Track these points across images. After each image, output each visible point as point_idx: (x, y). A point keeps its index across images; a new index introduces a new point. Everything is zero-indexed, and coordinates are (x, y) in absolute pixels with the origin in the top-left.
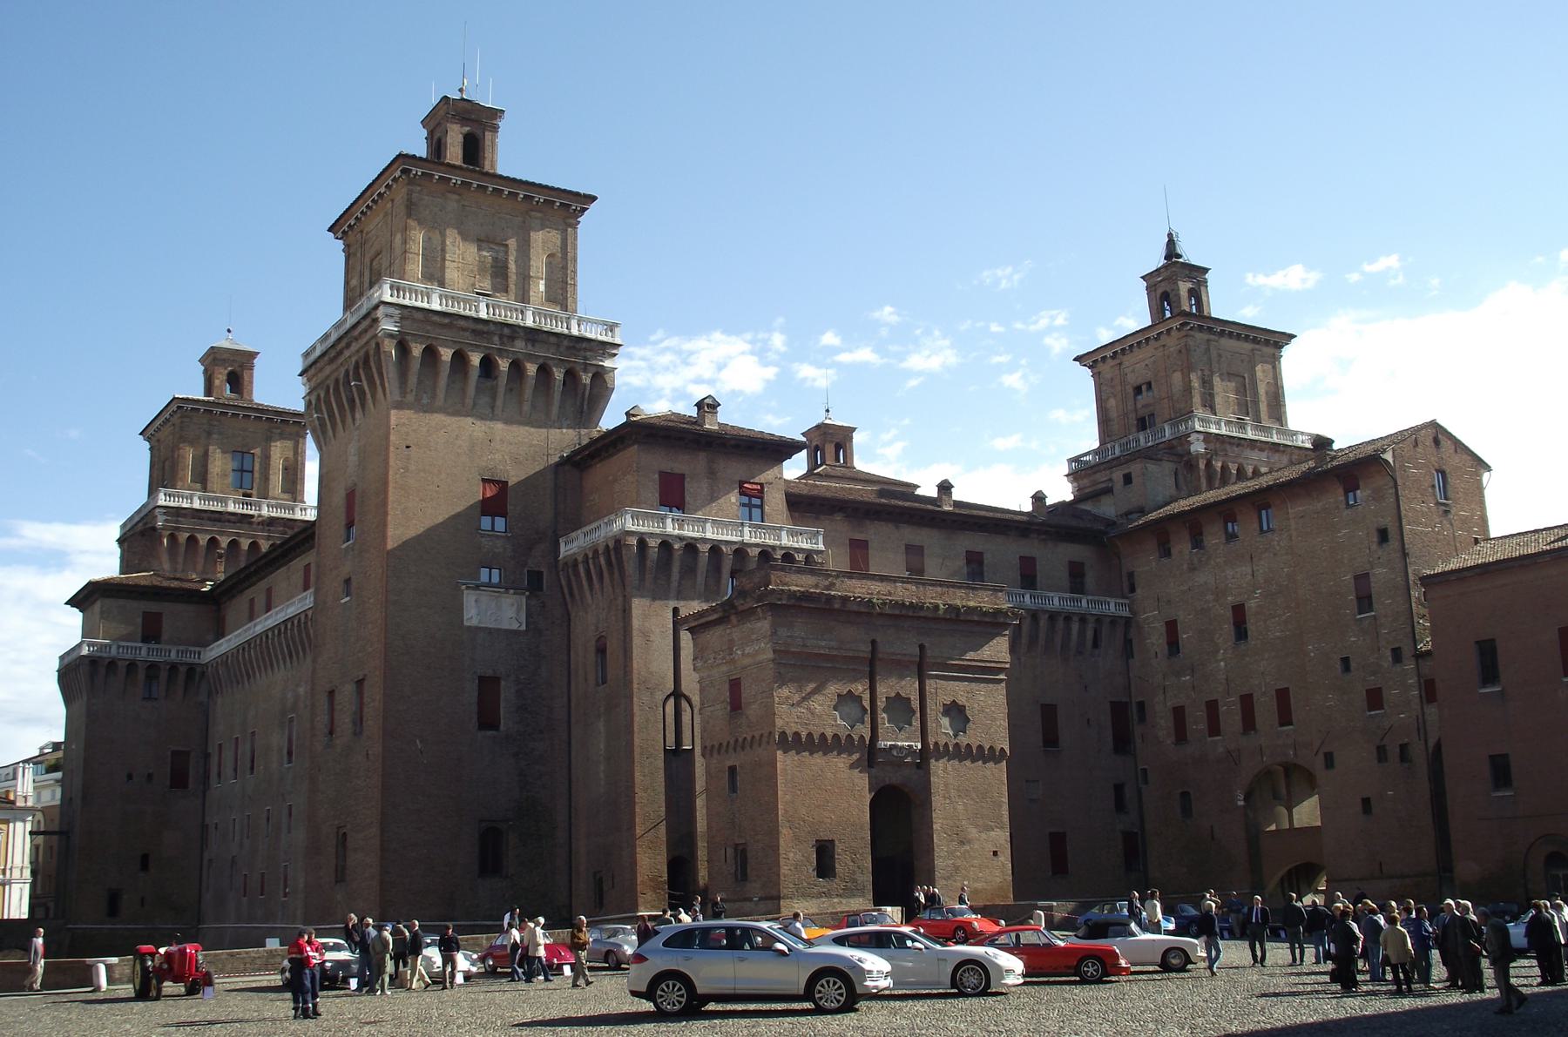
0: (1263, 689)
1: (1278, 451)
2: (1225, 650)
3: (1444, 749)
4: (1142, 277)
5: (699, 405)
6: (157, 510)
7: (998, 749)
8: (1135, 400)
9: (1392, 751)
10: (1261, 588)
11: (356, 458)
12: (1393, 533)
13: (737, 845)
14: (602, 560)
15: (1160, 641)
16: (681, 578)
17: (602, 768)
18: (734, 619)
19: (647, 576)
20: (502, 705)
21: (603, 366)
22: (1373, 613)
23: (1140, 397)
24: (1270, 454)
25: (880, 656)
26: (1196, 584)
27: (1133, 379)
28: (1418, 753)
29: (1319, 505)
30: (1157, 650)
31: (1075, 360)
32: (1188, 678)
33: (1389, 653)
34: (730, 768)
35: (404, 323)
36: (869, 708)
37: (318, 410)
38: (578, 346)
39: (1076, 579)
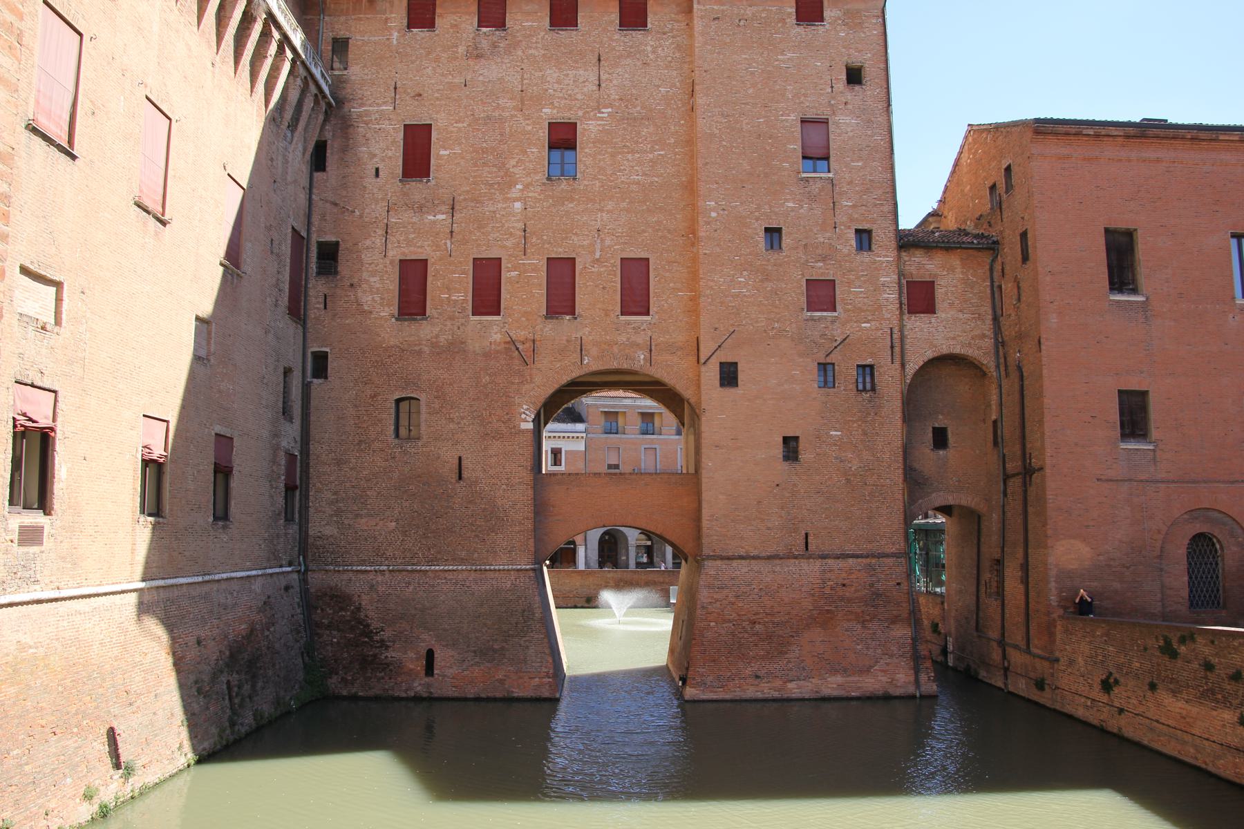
0: (597, 255)
2: (527, 186)
10: (611, 106)
12: (870, 73)
15: (390, 153)
22: (831, 175)
26: (481, 78)
28: (891, 382)
29: (749, 12)
30: (381, 166)
33: (852, 235)
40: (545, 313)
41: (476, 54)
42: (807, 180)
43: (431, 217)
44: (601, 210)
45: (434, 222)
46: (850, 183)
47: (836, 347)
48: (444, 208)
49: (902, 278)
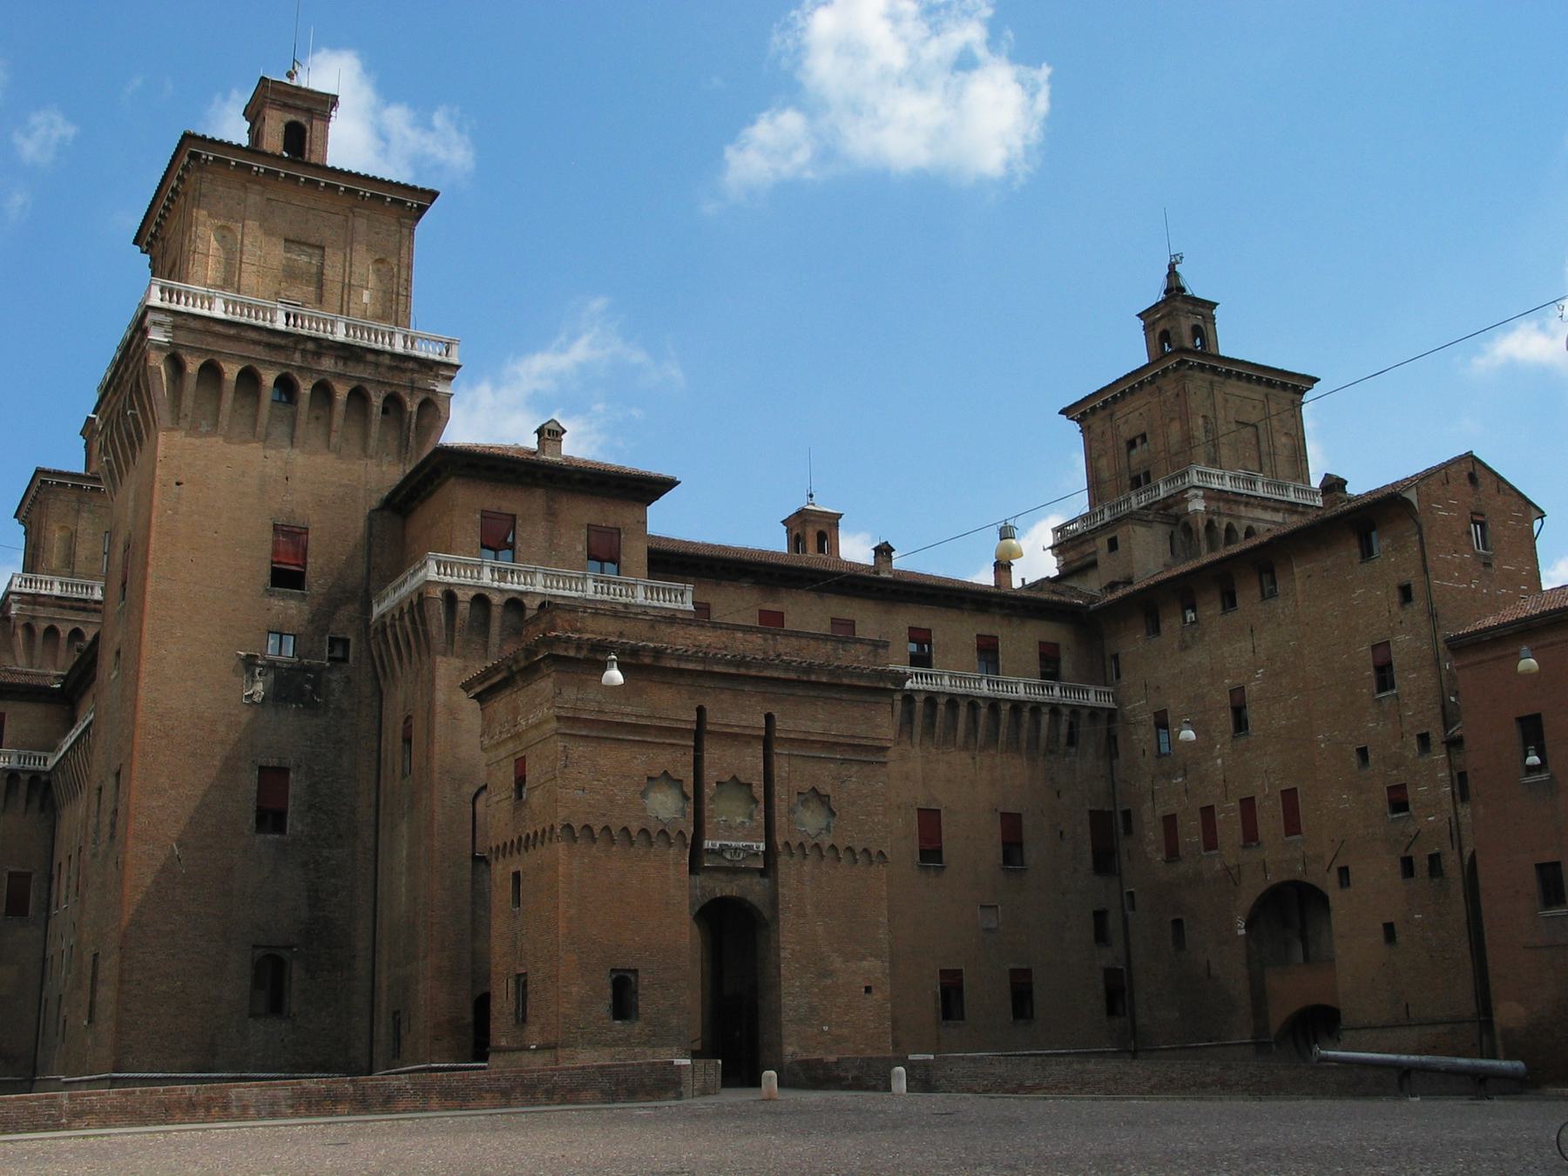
1: (1296, 512)
2: (1221, 746)
3: (1478, 857)
4: (1138, 315)
5: (540, 432)
6: (11, 597)
7: (874, 851)
8: (1129, 456)
9: (1421, 864)
11: (133, 503)
13: (519, 976)
14: (407, 619)
16: (502, 640)
17: (404, 881)
18: (518, 677)
19: (457, 638)
20: (290, 803)
21: (435, 390)
22: (1395, 692)
23: (1134, 452)
24: (1286, 515)
25: (708, 727)
26: (1189, 665)
27: (1127, 432)
31: (1061, 412)
32: (1180, 780)
33: (1414, 741)
34: (513, 874)
35: (177, 332)
36: (691, 795)
37: (106, 454)
38: (402, 365)
39: (1049, 667)
40: (1241, 843)
41: (1184, 647)
42: (1379, 700)
43: (1174, 781)
44: (1265, 754)
45: (1176, 784)
46: (1409, 695)
47: (1412, 842)
48: (1181, 772)
49: (1453, 771)
